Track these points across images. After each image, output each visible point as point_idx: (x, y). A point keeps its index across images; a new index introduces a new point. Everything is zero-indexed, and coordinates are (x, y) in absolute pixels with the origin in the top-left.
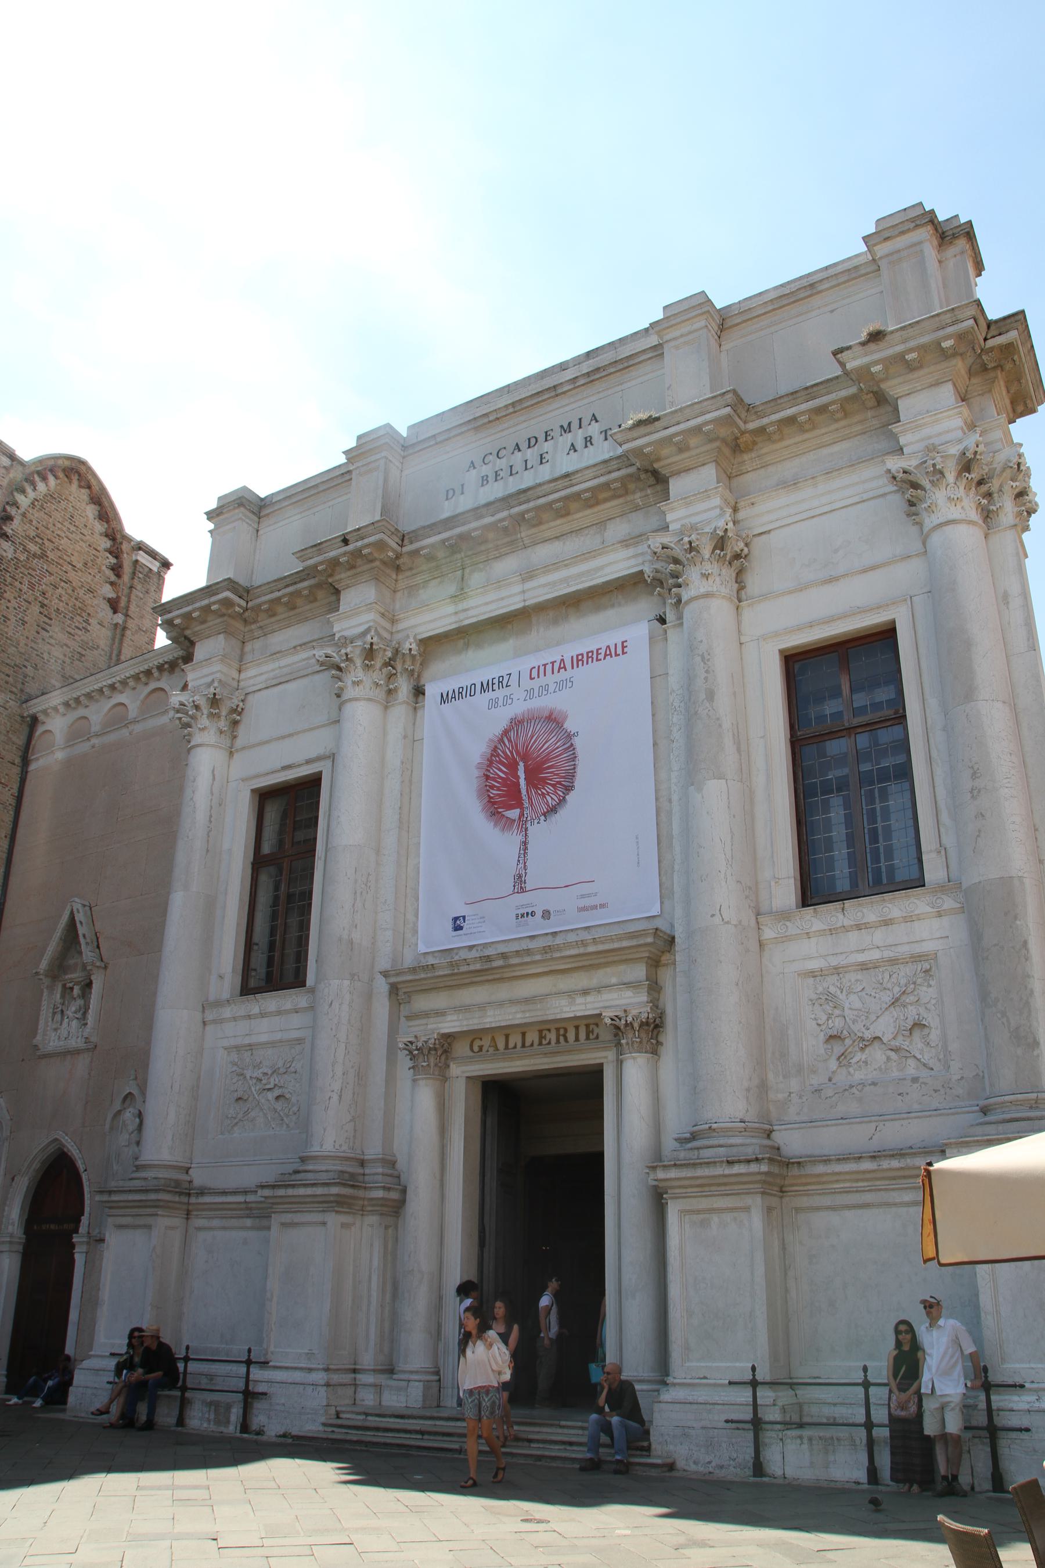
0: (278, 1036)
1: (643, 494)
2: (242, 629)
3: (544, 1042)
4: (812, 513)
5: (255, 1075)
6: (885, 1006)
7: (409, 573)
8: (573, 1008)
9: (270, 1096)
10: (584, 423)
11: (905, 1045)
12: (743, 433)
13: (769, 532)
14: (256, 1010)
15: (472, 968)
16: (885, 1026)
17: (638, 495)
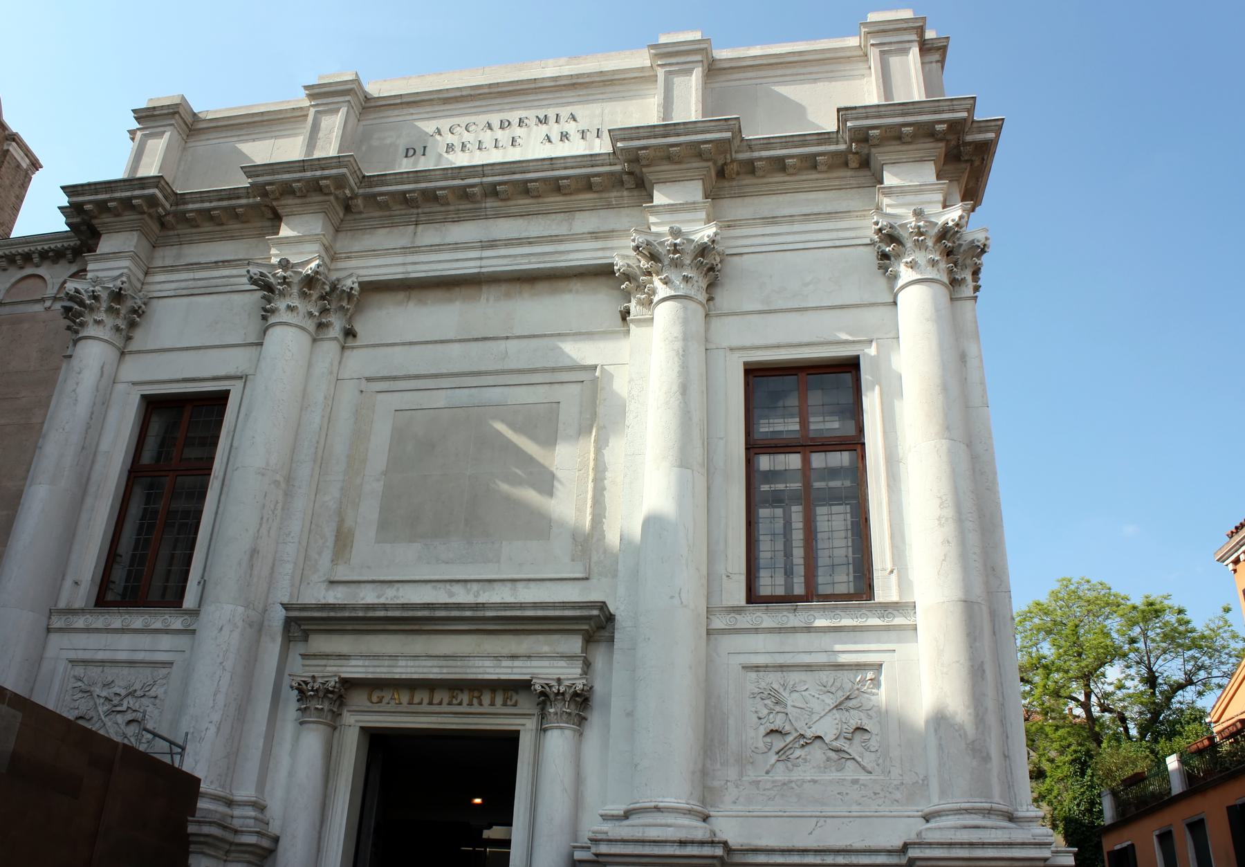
0: (140, 656)
1: (619, 194)
2: (157, 231)
3: (455, 702)
4: (785, 247)
5: (104, 694)
6: (828, 708)
7: (357, 216)
8: (498, 670)
9: (120, 719)
10: (562, 120)
11: (846, 747)
12: (733, 161)
13: (741, 254)
15: (390, 614)
16: (827, 727)
17: (614, 194)
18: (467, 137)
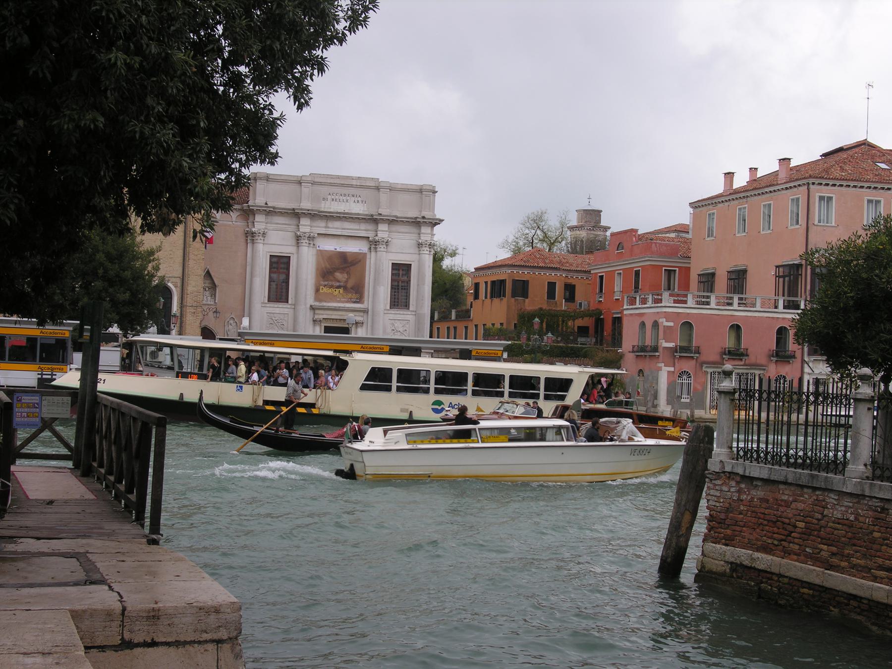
14: (276, 306)
16: (401, 330)
18: (337, 197)
